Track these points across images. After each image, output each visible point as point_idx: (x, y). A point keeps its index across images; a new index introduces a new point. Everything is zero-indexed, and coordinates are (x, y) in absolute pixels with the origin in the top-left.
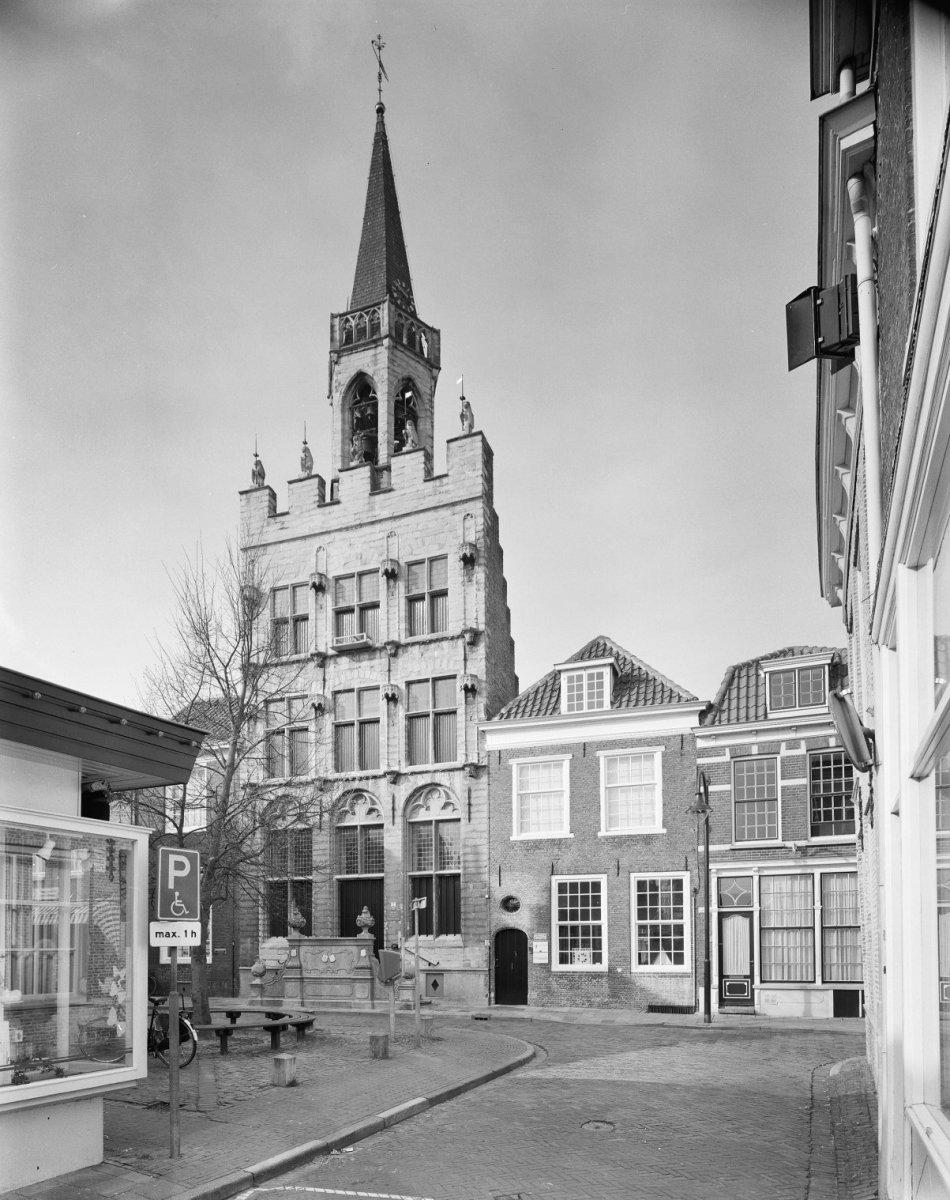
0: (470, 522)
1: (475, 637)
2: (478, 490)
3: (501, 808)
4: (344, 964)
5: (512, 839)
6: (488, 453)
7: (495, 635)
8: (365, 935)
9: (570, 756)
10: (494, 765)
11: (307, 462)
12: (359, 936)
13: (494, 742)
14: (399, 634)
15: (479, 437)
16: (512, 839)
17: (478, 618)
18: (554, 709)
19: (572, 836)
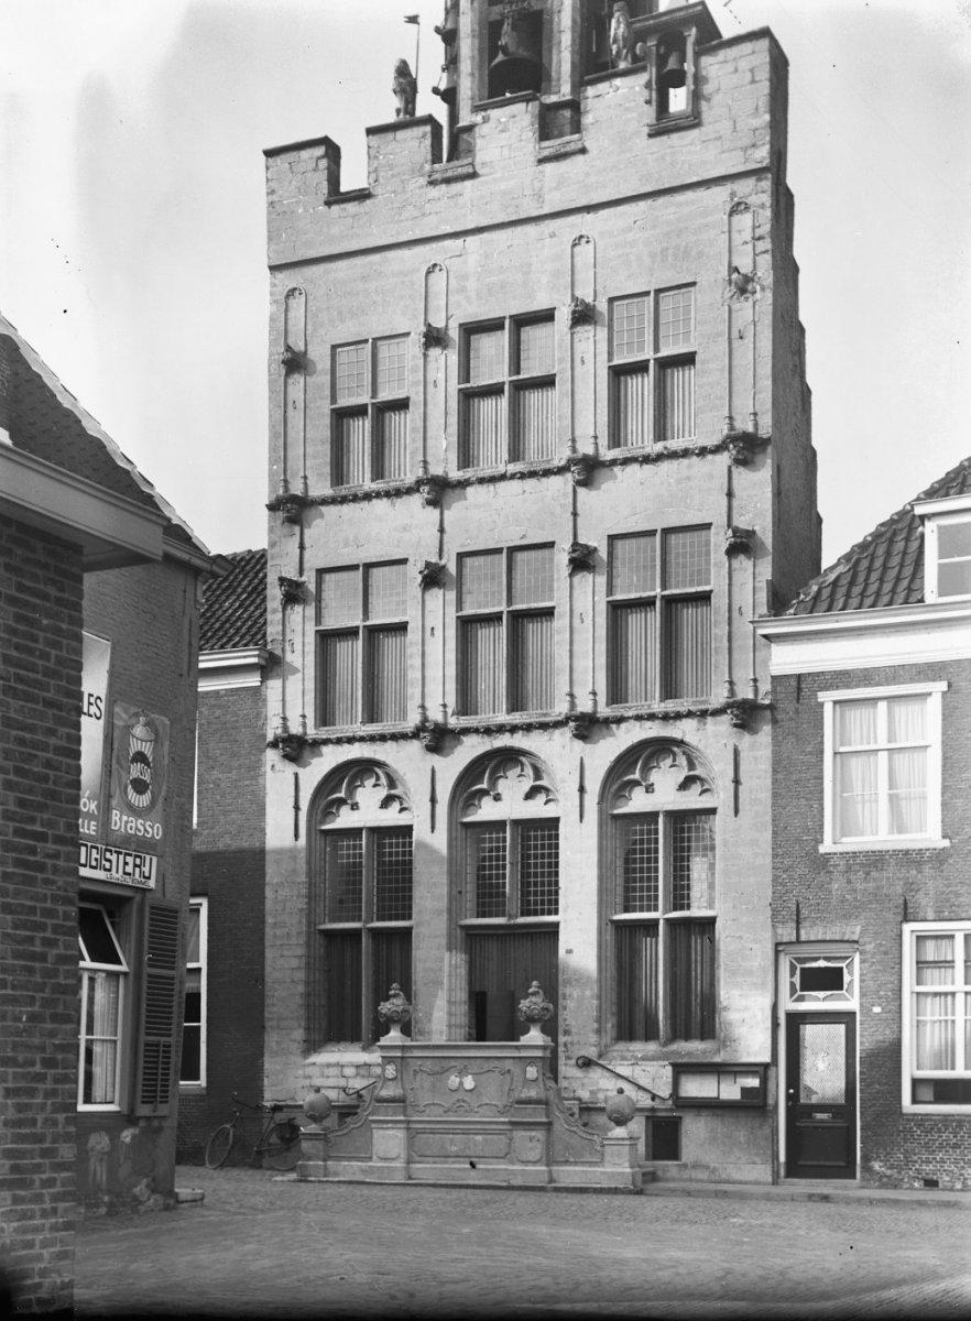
0: (744, 221)
1: (746, 448)
2: (762, 155)
3: (798, 783)
4: (494, 1094)
5: (822, 849)
6: (779, 65)
7: (782, 445)
8: (535, 1036)
9: (943, 686)
10: (787, 705)
11: (406, 83)
12: (525, 1040)
13: (788, 659)
14: (590, 433)
15: (764, 43)
16: (822, 849)
17: (756, 409)
18: (909, 590)
19: (946, 843)
